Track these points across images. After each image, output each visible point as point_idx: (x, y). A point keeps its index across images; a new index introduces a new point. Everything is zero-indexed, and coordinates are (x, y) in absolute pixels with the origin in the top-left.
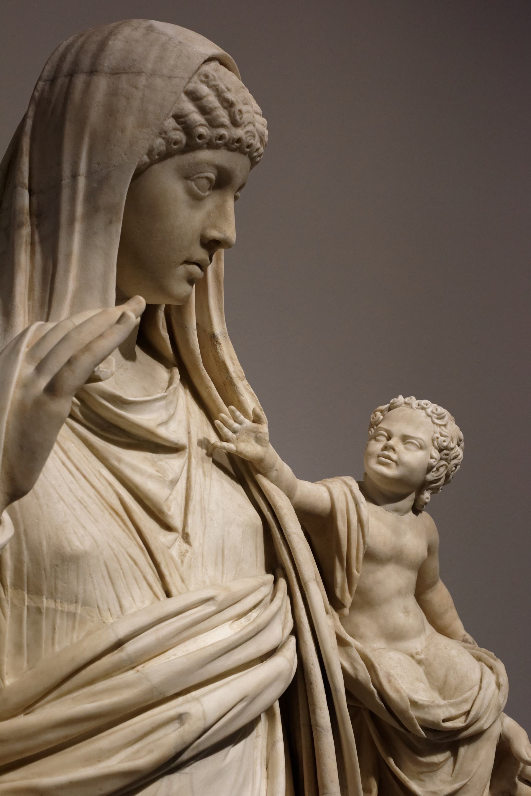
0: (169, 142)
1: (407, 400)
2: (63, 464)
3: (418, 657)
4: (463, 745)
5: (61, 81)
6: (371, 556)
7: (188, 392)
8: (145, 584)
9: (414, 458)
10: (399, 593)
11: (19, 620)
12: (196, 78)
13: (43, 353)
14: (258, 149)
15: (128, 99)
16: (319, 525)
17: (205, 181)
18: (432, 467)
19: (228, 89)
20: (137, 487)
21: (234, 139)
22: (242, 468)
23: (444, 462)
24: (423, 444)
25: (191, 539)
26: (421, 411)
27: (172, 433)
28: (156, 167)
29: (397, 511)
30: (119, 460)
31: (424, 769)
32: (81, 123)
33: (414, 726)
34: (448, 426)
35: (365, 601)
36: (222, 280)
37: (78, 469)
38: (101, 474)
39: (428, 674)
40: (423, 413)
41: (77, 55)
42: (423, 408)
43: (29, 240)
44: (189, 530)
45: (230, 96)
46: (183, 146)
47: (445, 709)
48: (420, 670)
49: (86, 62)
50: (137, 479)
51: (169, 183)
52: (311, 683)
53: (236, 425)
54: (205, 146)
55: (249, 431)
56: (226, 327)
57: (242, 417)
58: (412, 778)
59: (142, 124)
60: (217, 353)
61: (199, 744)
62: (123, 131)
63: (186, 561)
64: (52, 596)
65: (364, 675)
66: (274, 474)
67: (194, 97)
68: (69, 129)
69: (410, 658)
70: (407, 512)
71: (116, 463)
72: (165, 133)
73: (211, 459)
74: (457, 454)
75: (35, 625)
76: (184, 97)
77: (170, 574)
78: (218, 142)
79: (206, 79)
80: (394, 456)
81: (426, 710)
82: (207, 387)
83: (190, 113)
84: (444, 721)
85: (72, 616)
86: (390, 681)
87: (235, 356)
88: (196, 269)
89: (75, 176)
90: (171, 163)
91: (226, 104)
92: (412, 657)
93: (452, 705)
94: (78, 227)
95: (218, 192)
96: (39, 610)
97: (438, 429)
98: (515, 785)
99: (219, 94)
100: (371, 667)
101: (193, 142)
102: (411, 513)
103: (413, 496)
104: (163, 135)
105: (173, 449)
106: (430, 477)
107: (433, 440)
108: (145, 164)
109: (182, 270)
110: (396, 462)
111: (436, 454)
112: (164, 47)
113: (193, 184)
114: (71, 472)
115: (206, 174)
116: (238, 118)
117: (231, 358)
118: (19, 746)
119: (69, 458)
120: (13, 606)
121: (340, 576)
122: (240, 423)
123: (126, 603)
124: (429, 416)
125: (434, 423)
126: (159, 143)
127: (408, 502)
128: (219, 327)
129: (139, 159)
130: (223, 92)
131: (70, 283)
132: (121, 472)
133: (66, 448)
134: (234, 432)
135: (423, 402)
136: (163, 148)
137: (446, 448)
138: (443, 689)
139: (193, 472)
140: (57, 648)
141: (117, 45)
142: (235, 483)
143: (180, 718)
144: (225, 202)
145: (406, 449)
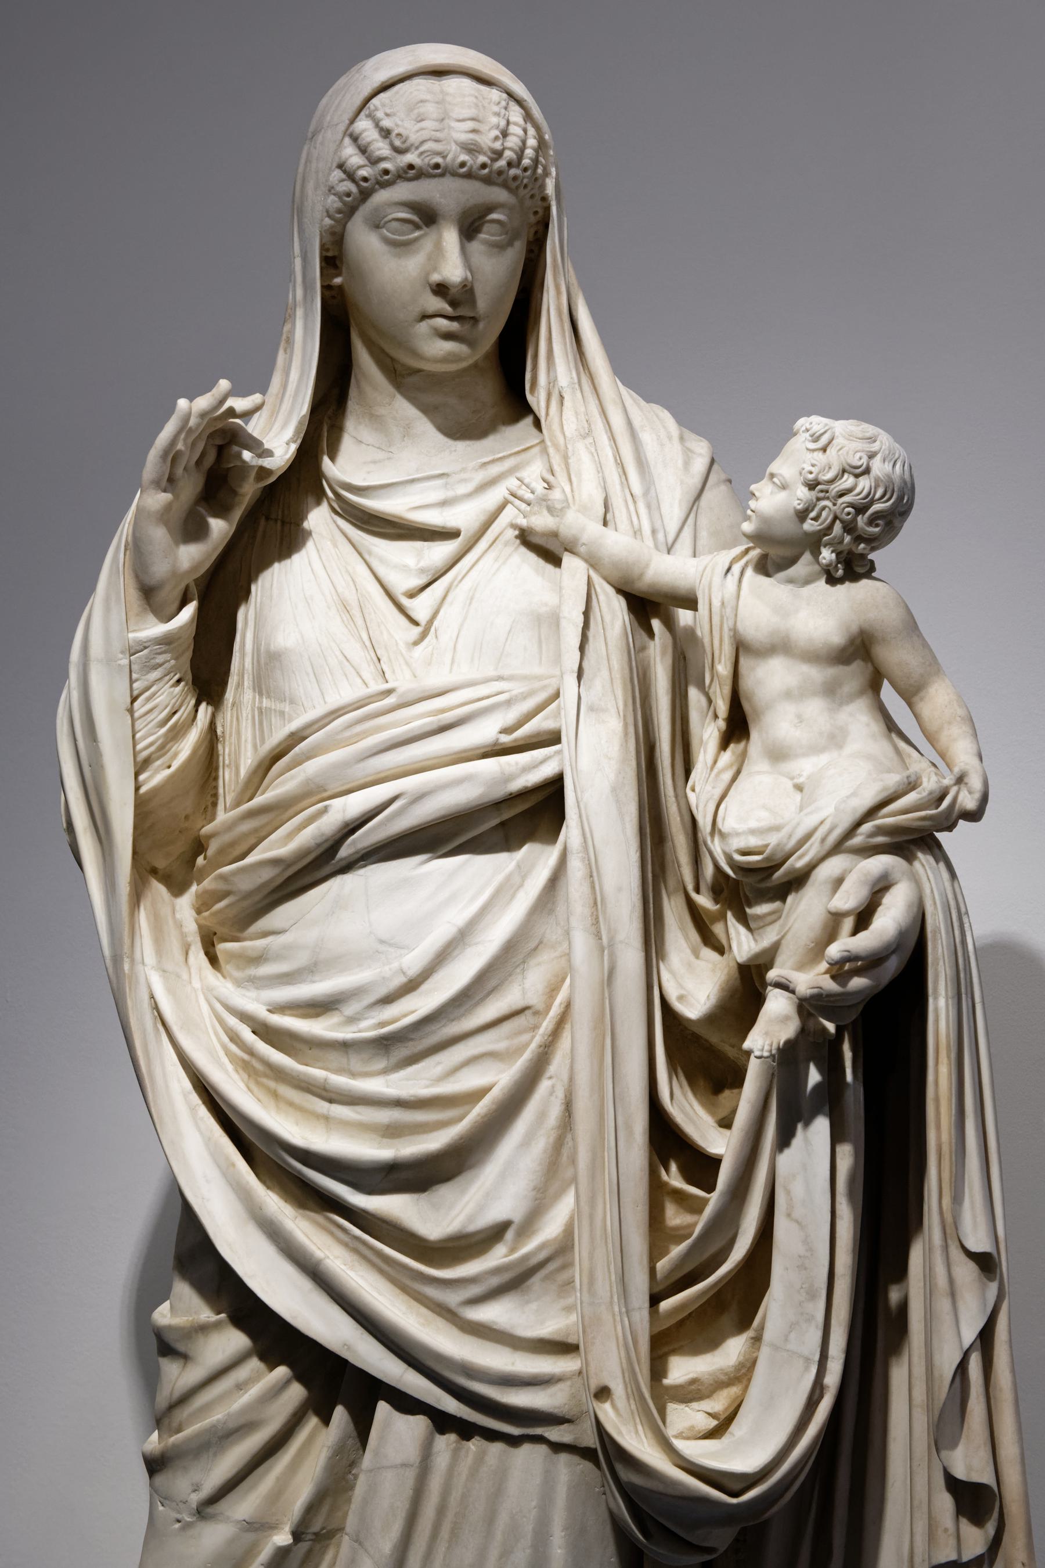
6: (741, 647)
8: (360, 681)
10: (788, 695)
14: (463, 165)
17: (395, 224)
19: (387, 115)
21: (402, 168)
28: (349, 225)
29: (790, 581)
30: (370, 553)
45: (386, 123)
46: (358, 195)
50: (381, 571)
53: (528, 496)
54: (377, 186)
61: (354, 842)
64: (269, 697)
66: (582, 550)
67: (355, 139)
70: (807, 581)
76: (347, 141)
77: (394, 672)
78: (386, 177)
83: (347, 159)
84: (745, 853)
85: (282, 713)
90: (358, 218)
95: (434, 227)
96: (260, 709)
97: (809, 455)
99: (377, 124)
102: (821, 584)
103: (807, 557)
105: (450, 534)
106: (809, 526)
108: (332, 227)
109: (424, 327)
111: (803, 493)
116: (397, 143)
129: (318, 225)
136: (338, 204)
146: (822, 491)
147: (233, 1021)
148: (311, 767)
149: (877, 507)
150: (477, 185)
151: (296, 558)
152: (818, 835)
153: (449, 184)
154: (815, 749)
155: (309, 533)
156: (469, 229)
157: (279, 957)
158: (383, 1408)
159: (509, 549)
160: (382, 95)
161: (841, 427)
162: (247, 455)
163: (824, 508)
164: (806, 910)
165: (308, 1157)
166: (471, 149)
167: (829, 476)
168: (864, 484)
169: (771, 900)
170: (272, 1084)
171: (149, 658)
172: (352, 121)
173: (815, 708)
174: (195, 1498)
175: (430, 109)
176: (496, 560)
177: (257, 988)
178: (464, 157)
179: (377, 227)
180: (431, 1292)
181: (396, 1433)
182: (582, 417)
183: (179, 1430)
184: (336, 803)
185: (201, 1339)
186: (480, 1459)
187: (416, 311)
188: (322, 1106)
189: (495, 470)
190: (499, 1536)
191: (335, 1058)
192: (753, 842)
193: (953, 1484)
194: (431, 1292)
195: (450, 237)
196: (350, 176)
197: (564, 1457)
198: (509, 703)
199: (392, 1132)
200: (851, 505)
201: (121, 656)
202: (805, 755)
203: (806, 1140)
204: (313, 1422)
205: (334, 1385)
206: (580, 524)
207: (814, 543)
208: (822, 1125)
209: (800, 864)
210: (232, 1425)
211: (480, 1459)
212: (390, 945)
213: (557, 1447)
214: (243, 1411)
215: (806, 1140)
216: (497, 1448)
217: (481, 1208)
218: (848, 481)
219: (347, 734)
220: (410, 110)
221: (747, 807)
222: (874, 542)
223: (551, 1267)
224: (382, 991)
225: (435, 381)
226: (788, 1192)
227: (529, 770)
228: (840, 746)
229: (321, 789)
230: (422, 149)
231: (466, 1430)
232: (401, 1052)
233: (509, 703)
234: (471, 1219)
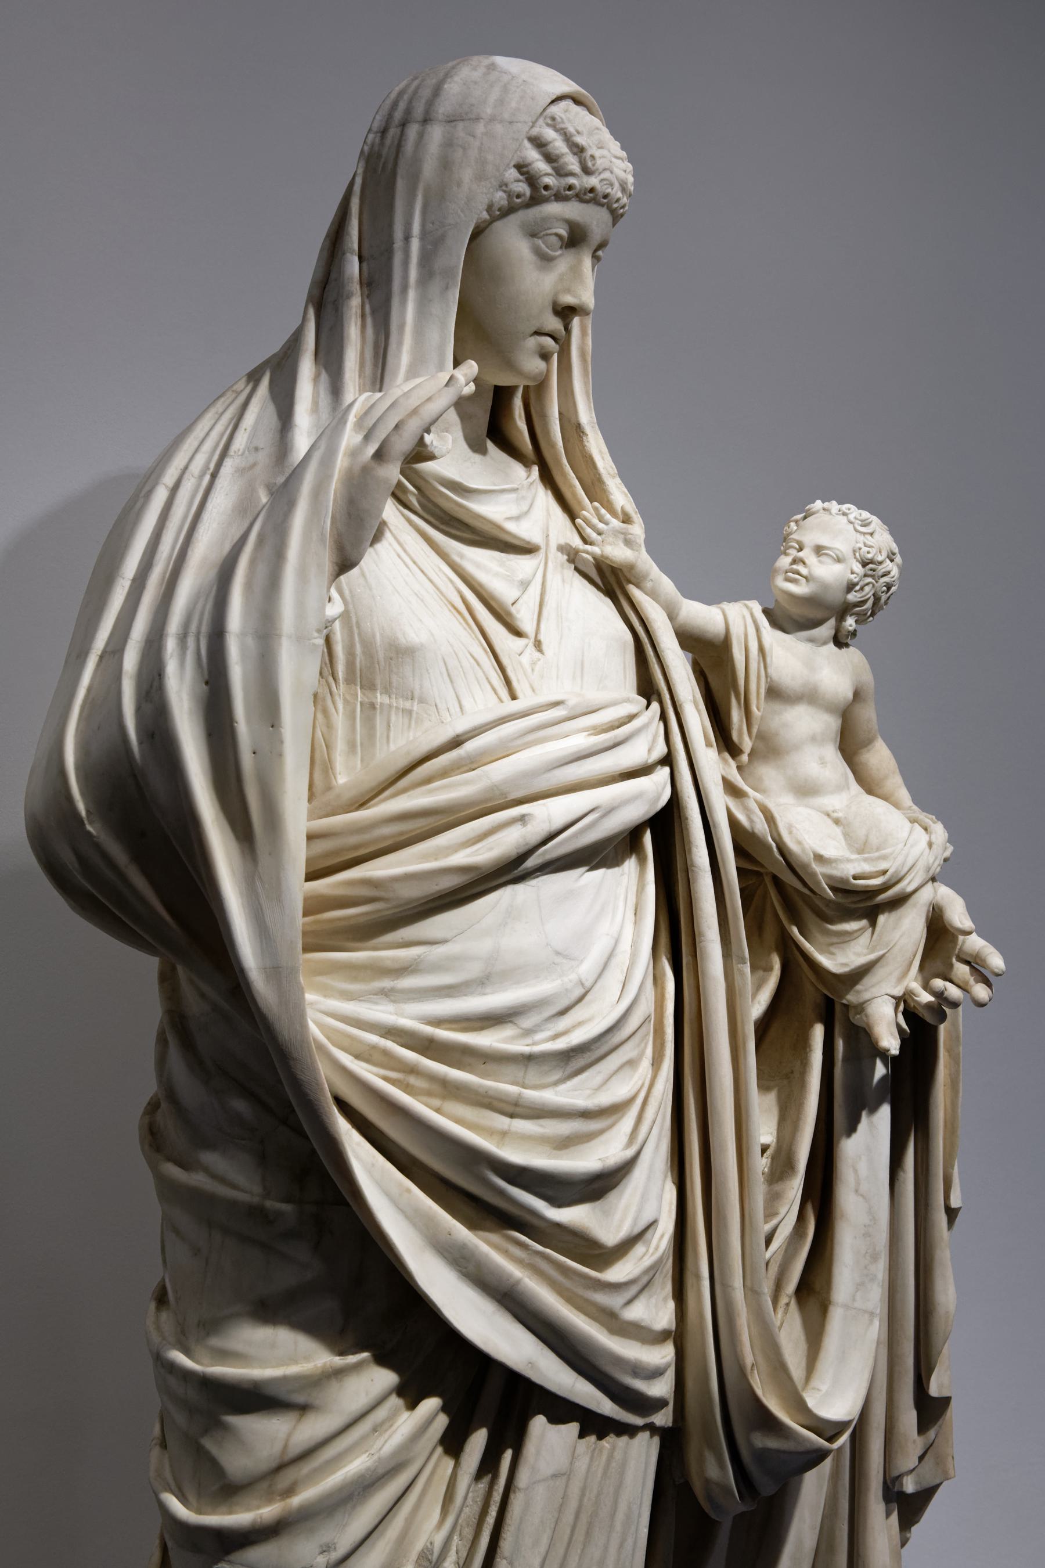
0: (509, 194)
1: (826, 505)
2: (399, 556)
3: (835, 815)
4: (883, 912)
5: (393, 132)
6: (774, 693)
7: (549, 493)
9: (829, 573)
10: (813, 739)
11: (352, 717)
12: (541, 121)
13: (370, 422)
14: (618, 200)
15: (464, 149)
16: (710, 657)
17: (554, 239)
18: (855, 585)
19: (578, 133)
20: (481, 585)
22: (612, 580)
23: (870, 580)
24: (840, 556)
25: (544, 647)
26: (841, 517)
27: (524, 530)
28: (498, 224)
29: (811, 640)
30: (462, 556)
31: (835, 940)
33: (818, 883)
34: (876, 536)
35: (769, 748)
36: (589, 360)
37: (415, 563)
38: (440, 570)
39: (846, 835)
40: (844, 519)
41: (410, 101)
42: (844, 514)
43: (359, 311)
44: (542, 637)
45: (579, 140)
47: (856, 864)
48: (837, 831)
49: (419, 111)
50: (482, 577)
51: (512, 242)
52: (687, 819)
53: (601, 526)
55: (616, 533)
56: (594, 415)
57: (608, 516)
58: (821, 951)
59: (480, 177)
60: (584, 446)
61: (546, 851)
62: (459, 185)
63: (537, 669)
64: (387, 690)
65: (761, 827)
66: (649, 585)
67: (539, 143)
68: (401, 185)
69: (826, 817)
70: (825, 643)
71: (456, 558)
72: (506, 185)
73: (573, 566)
74: (888, 569)
78: (568, 193)
79: (554, 123)
80: (804, 571)
81: (834, 865)
82: (571, 486)
84: (855, 878)
86: (790, 833)
87: (605, 450)
88: (548, 341)
89: (407, 238)
91: (575, 150)
92: (828, 815)
93: (865, 860)
94: (412, 294)
95: (573, 250)
96: (373, 706)
97: (861, 538)
98: (951, 966)
99: (567, 138)
100: (770, 819)
101: (538, 194)
102: (831, 645)
103: (832, 622)
104: (504, 188)
105: (526, 549)
106: (852, 597)
107: (854, 551)
108: (485, 221)
109: (532, 342)
110: (806, 578)
111: (858, 568)
112: (505, 89)
113: (540, 242)
114: (407, 566)
115: (554, 231)
116: (590, 164)
117: (601, 452)
118: (353, 840)
119: (405, 551)
120: (346, 702)
121: (736, 716)
122: (607, 523)
123: (464, 703)
124: (851, 523)
125: (856, 531)
126: (500, 198)
127: (826, 630)
128: (586, 415)
130: (572, 136)
131: (403, 355)
132: (463, 569)
133: (401, 540)
134: (599, 534)
135: (845, 507)
136: (504, 203)
137: (872, 562)
138: (862, 848)
139: (549, 576)
140: (393, 747)
141: (453, 88)
142: (602, 595)
143: (522, 819)
144: (580, 262)
145: (820, 562)
146: (871, 570)
147: (373, 1038)
157: (436, 968)
158: (539, 1423)
163: (867, 584)
167: (880, 558)
169: (859, 918)
170: (437, 1102)
176: (563, 581)
177: (394, 1002)
178: (619, 194)
179: (533, 235)
180: (602, 1298)
183: (290, 1491)
187: (534, 326)
188: (502, 1122)
190: (618, 1526)
191: (511, 1070)
192: (867, 868)
194: (602, 1298)
201: (316, 634)
203: (872, 1126)
207: (844, 610)
208: (885, 1111)
209: (909, 889)
212: (566, 957)
214: (396, 1453)
215: (872, 1126)
218: (888, 565)
219: (519, 742)
226: (856, 1171)
228: (848, 789)
229: (504, 794)
230: (603, 176)
232: (580, 1062)
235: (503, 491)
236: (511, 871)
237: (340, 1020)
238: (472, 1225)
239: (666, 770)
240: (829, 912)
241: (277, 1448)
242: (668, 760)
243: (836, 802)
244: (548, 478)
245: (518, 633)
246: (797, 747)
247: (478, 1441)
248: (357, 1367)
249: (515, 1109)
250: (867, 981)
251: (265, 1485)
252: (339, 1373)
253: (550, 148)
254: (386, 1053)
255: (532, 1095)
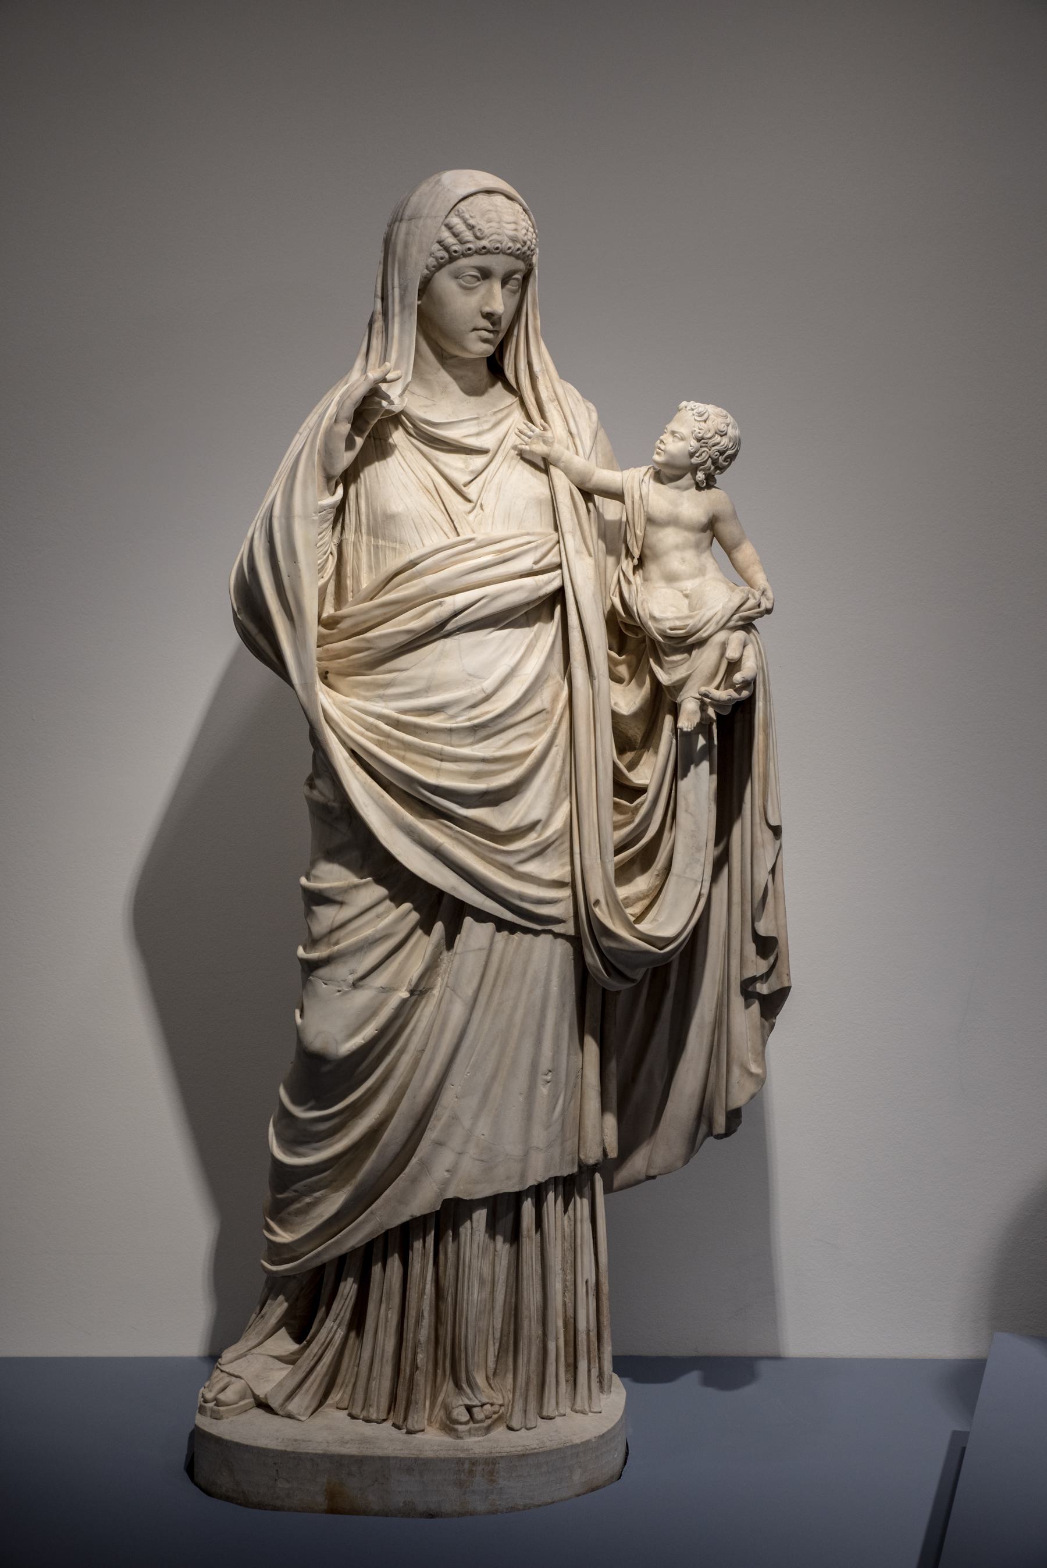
0: (436, 259)
10: (677, 547)
14: (509, 248)
28: (437, 274)
29: (678, 488)
30: (437, 460)
32: (394, 253)
40: (691, 413)
45: (472, 222)
48: (686, 601)
50: (447, 471)
51: (445, 284)
53: (530, 433)
64: (384, 539)
66: (562, 465)
67: (449, 227)
70: (687, 489)
75: (376, 554)
76: (443, 228)
80: (662, 447)
85: (394, 549)
94: (397, 319)
95: (487, 281)
96: (377, 547)
97: (697, 424)
99: (465, 221)
102: (694, 489)
103: (689, 475)
105: (485, 452)
106: (695, 460)
109: (474, 334)
111: (694, 443)
116: (478, 234)
118: (362, 618)
122: (532, 431)
126: (432, 261)
131: (394, 355)
136: (435, 263)
142: (538, 473)
144: (492, 286)
147: (371, 720)
148: (429, 580)
149: (729, 452)
150: (512, 259)
151: (389, 460)
152: (714, 620)
153: (502, 258)
154: (692, 576)
155: (395, 446)
156: (504, 283)
157: (403, 683)
158: (468, 921)
159: (514, 462)
160: (463, 203)
161: (711, 409)
162: (384, 403)
164: (706, 659)
165: (436, 790)
166: (514, 240)
167: (709, 435)
168: (725, 441)
169: (683, 653)
170: (402, 753)
171: (325, 516)
172: (446, 217)
173: (690, 554)
174: (351, 978)
175: (493, 215)
178: (510, 244)
179: (457, 278)
180: (500, 858)
181: (475, 935)
182: (551, 390)
183: (337, 943)
184: (448, 599)
185: (354, 891)
186: (520, 943)
188: (437, 763)
189: (500, 416)
191: (444, 737)
192: (678, 623)
193: (757, 938)
194: (500, 858)
195: (497, 286)
196: (446, 249)
197: (559, 941)
198: (536, 548)
199: (476, 776)
200: (718, 451)
202: (688, 579)
203: (697, 774)
204: (419, 932)
205: (439, 911)
206: (561, 449)
207: (694, 469)
208: (705, 765)
209: (705, 635)
210: (377, 936)
211: (520, 943)
213: (557, 935)
215: (697, 774)
216: (529, 936)
217: (526, 814)
218: (717, 439)
220: (483, 215)
221: (661, 606)
222: (722, 469)
223: (557, 843)
224: (472, 701)
225: (464, 363)
226: (686, 799)
227: (549, 583)
228: (704, 575)
229: (434, 591)
231: (512, 928)
233: (536, 548)
234: (522, 819)
235: (463, 421)
236: (437, 631)
237: (345, 710)
238: (422, 816)
239: (559, 571)
240: (667, 650)
241: (329, 923)
242: (559, 566)
243: (689, 585)
244: (523, 404)
245: (470, 501)
246: (666, 553)
247: (439, 927)
248: (365, 884)
249: (442, 757)
250: (684, 689)
251: (326, 940)
252: (356, 887)
253: (454, 230)
254: (377, 727)
255: (448, 749)
